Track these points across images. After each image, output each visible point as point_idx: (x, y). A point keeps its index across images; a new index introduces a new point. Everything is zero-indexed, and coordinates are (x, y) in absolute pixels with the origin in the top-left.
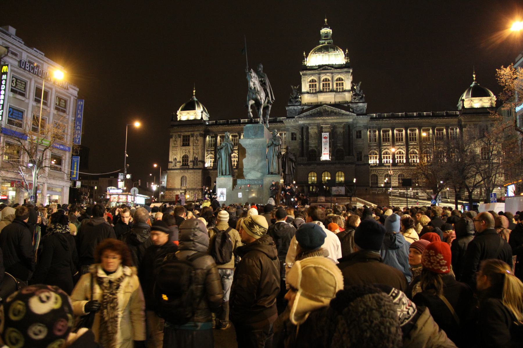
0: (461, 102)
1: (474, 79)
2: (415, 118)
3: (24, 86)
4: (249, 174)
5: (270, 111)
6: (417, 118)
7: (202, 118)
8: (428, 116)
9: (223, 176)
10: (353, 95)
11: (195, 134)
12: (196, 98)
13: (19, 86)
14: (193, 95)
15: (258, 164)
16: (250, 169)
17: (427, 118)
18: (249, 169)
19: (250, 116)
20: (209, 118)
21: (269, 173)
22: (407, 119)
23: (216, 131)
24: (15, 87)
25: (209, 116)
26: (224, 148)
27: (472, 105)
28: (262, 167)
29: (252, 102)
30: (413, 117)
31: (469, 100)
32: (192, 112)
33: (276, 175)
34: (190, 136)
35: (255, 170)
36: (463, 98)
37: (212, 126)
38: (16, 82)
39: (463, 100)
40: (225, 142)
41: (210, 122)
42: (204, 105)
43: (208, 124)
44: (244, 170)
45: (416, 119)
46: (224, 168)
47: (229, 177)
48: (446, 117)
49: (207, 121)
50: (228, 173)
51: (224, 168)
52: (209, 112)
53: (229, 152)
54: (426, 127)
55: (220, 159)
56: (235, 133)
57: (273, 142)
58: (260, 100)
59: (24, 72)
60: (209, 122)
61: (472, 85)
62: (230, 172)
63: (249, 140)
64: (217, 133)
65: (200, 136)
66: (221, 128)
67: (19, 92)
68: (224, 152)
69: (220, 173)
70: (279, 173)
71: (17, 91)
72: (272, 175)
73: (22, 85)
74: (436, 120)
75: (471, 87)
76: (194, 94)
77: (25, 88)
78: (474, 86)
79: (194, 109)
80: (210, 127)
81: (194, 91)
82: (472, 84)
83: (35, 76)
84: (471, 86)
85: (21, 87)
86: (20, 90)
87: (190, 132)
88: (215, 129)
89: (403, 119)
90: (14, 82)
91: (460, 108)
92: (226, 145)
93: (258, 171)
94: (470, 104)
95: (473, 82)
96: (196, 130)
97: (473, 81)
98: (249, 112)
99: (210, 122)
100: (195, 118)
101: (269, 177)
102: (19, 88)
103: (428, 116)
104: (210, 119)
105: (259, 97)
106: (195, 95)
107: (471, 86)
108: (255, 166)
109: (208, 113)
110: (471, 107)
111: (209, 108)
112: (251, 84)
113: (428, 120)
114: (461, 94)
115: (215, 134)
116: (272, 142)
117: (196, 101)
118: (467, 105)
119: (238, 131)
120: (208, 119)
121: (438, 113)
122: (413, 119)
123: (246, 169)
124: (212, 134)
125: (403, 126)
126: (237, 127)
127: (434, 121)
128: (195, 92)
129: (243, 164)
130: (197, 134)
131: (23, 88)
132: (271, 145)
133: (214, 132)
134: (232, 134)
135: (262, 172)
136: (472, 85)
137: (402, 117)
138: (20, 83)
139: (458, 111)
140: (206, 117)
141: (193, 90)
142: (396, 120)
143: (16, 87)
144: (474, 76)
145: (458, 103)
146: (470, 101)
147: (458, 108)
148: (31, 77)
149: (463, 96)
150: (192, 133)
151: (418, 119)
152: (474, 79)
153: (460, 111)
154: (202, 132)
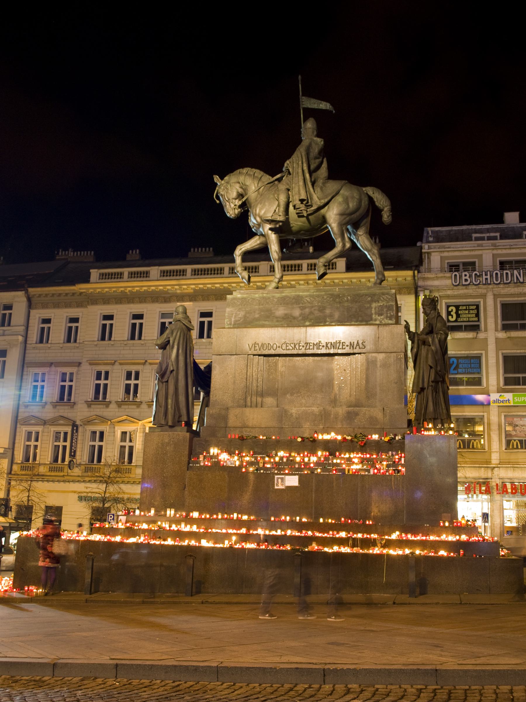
3: (476, 311)
13: (465, 316)
24: (456, 321)
38: (457, 313)
59: (466, 289)
67: (465, 326)
71: (461, 326)
73: (471, 312)
77: (478, 315)
83: (490, 286)
85: (469, 316)
86: (469, 321)
90: (453, 313)
102: (465, 319)
131: (474, 315)
138: (466, 310)
143: (459, 320)
148: (484, 291)
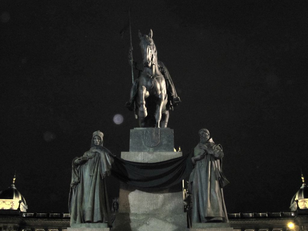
0: (295, 202)
1: (303, 181)
2: (251, 219)
4: (144, 226)
5: (166, 124)
6: (254, 219)
7: (19, 209)
8: (264, 217)
9: (84, 225)
10: (187, 193)
11: (8, 226)
12: (15, 187)
14: (12, 183)
15: (164, 204)
16: (148, 214)
17: (264, 219)
18: (143, 214)
19: (143, 112)
20: (26, 210)
21: (200, 220)
22: (244, 220)
23: (34, 225)
25: (27, 208)
26: (90, 162)
27: (306, 206)
28: (174, 212)
29: (145, 93)
30: (248, 218)
31: (302, 201)
32: (8, 201)
33: (219, 224)
34: (3, 229)
35: (158, 218)
36: (296, 199)
37: (30, 219)
39: (297, 201)
40: (94, 151)
41: (28, 214)
42: (23, 196)
43: (24, 216)
44: (132, 218)
45: (252, 220)
46: (87, 206)
47: (99, 227)
48: (282, 219)
49: (24, 213)
50: (97, 217)
51: (87, 206)
52: (28, 204)
53: (101, 170)
54: (263, 228)
55: (80, 186)
56: (56, 229)
57: (205, 150)
58: (160, 92)
60: (26, 215)
61: (303, 186)
62: (102, 216)
63: (142, 154)
64: (35, 227)
65: (14, 229)
66: (40, 222)
68: (91, 170)
69: (75, 219)
70: (224, 221)
72: (210, 224)
74: (273, 221)
75: (302, 189)
76: (14, 182)
78: (304, 188)
79: (12, 198)
80: (27, 220)
81: (14, 179)
82: (301, 186)
84: (301, 188)
87: (2, 223)
88: (32, 222)
89: (239, 220)
91: (294, 209)
92: (95, 156)
93: (164, 220)
94: (303, 205)
95: (302, 184)
96: (11, 221)
97: (302, 183)
98: (143, 104)
99: (28, 214)
100: (11, 208)
101: (203, 228)
103: (264, 217)
104: (28, 211)
105: (158, 86)
106: (15, 184)
107: (301, 188)
108: (157, 209)
109: (27, 204)
110: (305, 208)
111: (28, 199)
112: (149, 56)
113: (265, 221)
114: (293, 195)
115: (31, 229)
116: (202, 152)
117: (15, 190)
118: (301, 206)
119: (59, 227)
120: (25, 211)
121: (274, 214)
122: (250, 220)
123: (136, 215)
124: (28, 228)
125: (240, 227)
126: (59, 222)
127: (271, 222)
128: (15, 180)
129: (129, 204)
130: (11, 227)
132: (202, 157)
133: (30, 226)
134: (51, 230)
135: (173, 223)
136: (303, 186)
137: (238, 218)
139: (292, 212)
140: (23, 208)
141: (14, 178)
142: (232, 221)
144: (303, 178)
145: (290, 205)
146: (303, 202)
147: (290, 209)
149: (295, 197)
150: (5, 225)
151: (254, 220)
152: (303, 181)
153: (295, 212)
154: (17, 225)
